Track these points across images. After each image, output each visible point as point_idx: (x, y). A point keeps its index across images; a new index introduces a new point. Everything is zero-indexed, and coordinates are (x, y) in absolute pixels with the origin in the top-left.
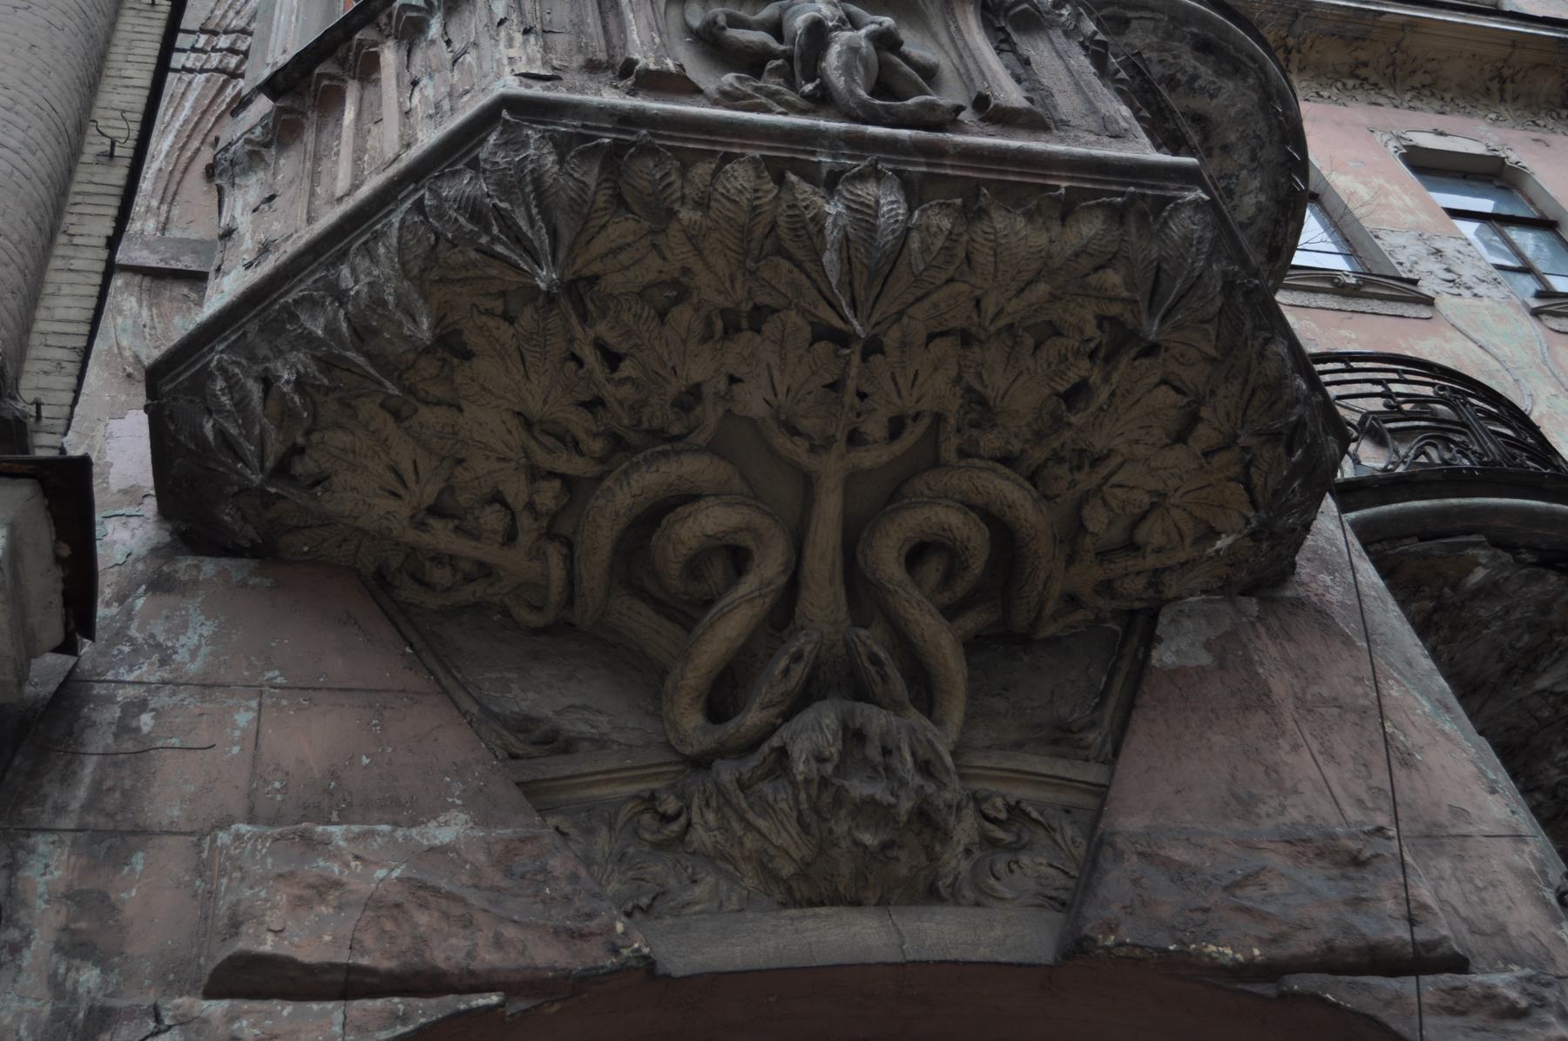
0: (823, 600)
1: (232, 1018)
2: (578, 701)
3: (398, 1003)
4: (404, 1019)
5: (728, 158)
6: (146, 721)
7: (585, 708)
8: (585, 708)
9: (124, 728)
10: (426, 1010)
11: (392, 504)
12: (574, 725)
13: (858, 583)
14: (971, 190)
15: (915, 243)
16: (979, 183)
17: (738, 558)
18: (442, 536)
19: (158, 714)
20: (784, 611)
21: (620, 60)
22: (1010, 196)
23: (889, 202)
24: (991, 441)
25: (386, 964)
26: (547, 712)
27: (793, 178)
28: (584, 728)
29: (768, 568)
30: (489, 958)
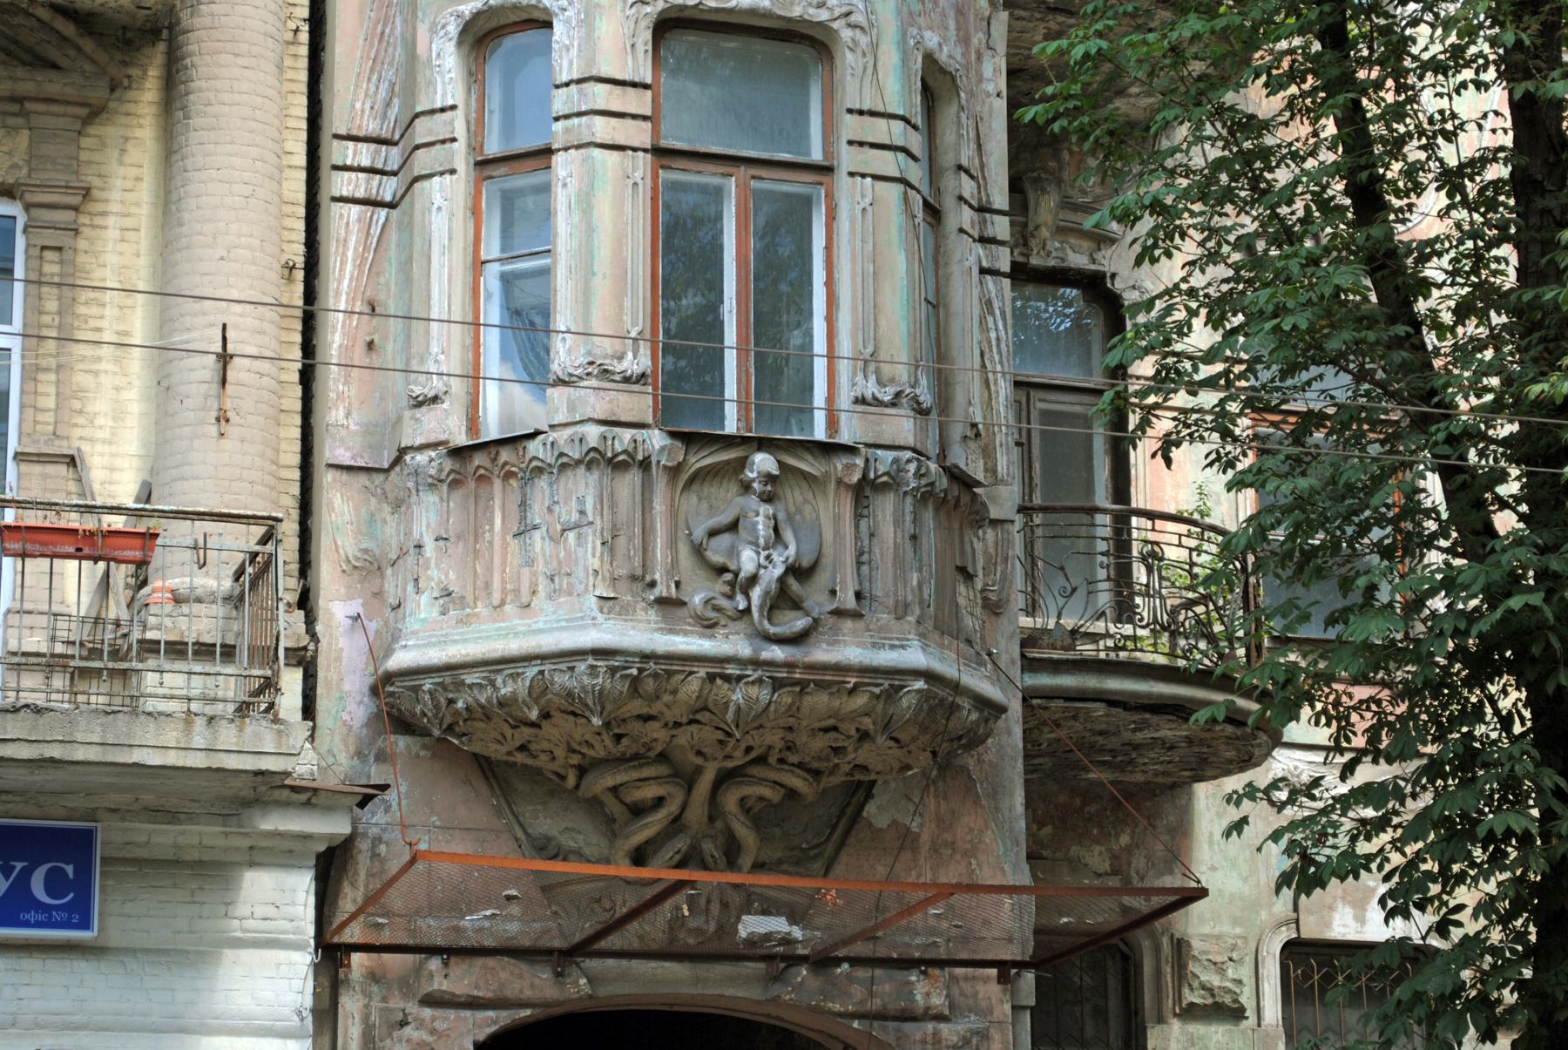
0: (697, 812)
1: (434, 1019)
2: (570, 825)
3: (491, 1013)
4: (494, 1022)
5: (691, 673)
6: (382, 849)
7: (573, 830)
8: (573, 830)
9: (375, 855)
11: (498, 747)
12: (568, 842)
13: (714, 811)
14: (803, 684)
15: (772, 708)
16: (809, 681)
17: (659, 802)
18: (520, 758)
19: (387, 844)
20: (676, 824)
21: (648, 578)
22: (821, 685)
24: (794, 759)
25: (490, 995)
26: (554, 833)
27: (719, 682)
28: (572, 844)
29: (672, 808)
30: (528, 994)
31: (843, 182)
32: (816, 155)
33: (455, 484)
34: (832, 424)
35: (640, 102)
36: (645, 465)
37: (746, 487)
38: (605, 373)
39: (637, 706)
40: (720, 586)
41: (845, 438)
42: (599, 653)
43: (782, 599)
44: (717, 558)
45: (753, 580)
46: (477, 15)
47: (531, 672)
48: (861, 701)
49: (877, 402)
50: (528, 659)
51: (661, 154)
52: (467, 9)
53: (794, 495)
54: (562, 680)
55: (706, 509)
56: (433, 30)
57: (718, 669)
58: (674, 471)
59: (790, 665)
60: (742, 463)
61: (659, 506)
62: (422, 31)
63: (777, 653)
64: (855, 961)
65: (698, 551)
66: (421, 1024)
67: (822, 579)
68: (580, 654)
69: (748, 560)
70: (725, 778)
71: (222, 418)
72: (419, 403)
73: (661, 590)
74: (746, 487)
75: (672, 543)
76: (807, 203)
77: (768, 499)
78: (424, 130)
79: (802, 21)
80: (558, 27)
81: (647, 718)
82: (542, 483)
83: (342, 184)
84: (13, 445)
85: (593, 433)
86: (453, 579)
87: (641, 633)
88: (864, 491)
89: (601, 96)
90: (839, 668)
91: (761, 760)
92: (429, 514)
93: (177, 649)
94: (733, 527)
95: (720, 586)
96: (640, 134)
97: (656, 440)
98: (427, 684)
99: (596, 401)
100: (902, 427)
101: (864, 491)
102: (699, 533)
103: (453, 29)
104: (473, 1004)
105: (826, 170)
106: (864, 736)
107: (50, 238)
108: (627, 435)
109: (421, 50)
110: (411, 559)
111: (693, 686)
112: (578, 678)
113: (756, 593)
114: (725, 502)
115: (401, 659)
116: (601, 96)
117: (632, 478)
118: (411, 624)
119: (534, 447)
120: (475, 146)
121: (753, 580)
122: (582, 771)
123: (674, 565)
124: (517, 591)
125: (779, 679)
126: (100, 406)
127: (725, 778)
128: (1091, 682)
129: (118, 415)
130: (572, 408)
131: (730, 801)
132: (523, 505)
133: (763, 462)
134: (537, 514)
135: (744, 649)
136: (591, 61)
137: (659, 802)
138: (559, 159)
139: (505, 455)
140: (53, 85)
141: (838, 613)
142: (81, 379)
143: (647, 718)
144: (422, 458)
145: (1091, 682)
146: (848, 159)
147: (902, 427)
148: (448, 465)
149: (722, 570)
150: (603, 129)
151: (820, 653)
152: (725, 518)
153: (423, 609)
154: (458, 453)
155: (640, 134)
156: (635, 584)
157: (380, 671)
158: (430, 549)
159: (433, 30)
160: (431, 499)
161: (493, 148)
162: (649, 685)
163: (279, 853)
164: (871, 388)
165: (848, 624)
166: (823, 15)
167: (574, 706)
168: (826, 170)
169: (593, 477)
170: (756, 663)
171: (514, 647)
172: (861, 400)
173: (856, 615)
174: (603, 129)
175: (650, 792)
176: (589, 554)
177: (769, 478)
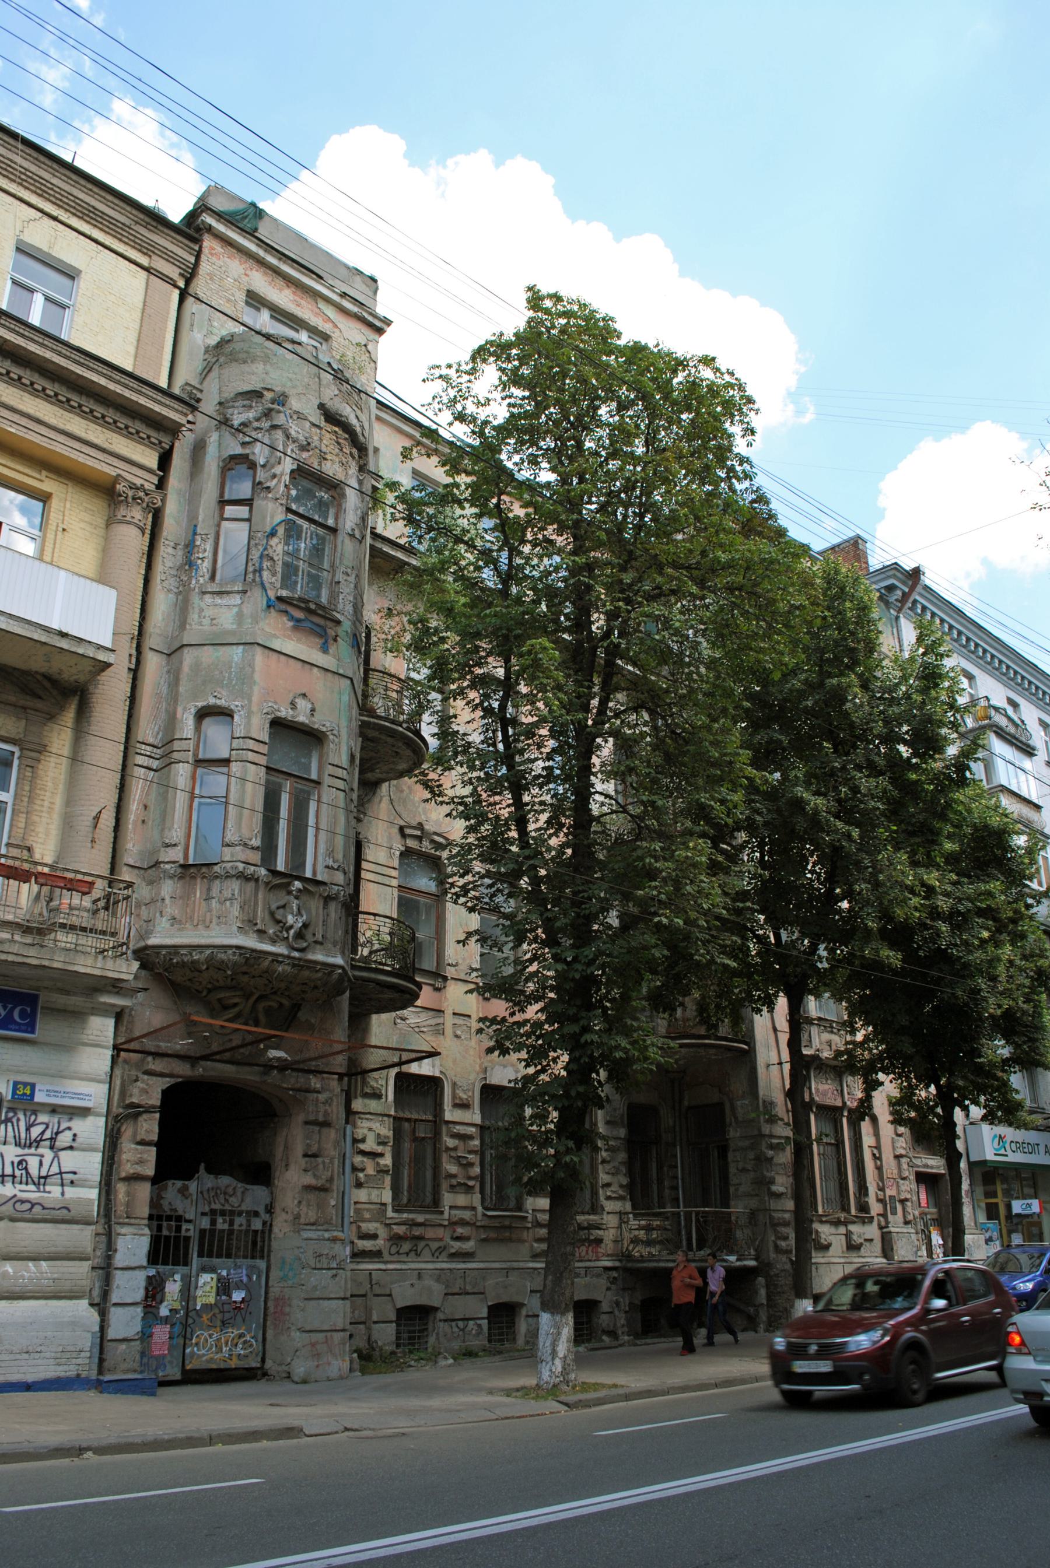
10: (173, 1081)
23: (288, 968)
31: (325, 788)
32: (314, 776)
33: (181, 878)
34: (314, 873)
35: (264, 749)
36: (257, 880)
37: (290, 893)
38: (245, 845)
39: (244, 969)
40: (278, 928)
41: (319, 878)
42: (238, 947)
43: (300, 935)
44: (279, 917)
45: (291, 927)
46: (203, 707)
47: (208, 952)
48: (320, 975)
49: (332, 868)
50: (208, 947)
51: (267, 768)
52: (200, 704)
53: (304, 898)
54: (222, 956)
55: (278, 899)
56: (185, 709)
57: (276, 957)
58: (267, 884)
59: (299, 959)
60: (289, 884)
61: (260, 896)
62: (180, 710)
63: (296, 954)
64: (293, 1070)
65: (272, 914)
66: (143, 1081)
67: (311, 930)
68: (230, 947)
69: (290, 919)
70: (261, 998)
71: (93, 841)
72: (168, 846)
73: (259, 927)
74: (290, 893)
75: (263, 911)
76: (309, 793)
77: (297, 898)
78: (177, 745)
79: (317, 730)
80: (236, 717)
81: (245, 973)
82: (217, 882)
83: (140, 760)
84: (5, 840)
85: (241, 866)
86: (176, 913)
87: (251, 942)
88: (327, 899)
89: (251, 744)
90: (316, 962)
91: (275, 993)
92: (168, 888)
93: (73, 928)
94: (284, 907)
95: (278, 928)
96: (263, 760)
97: (263, 871)
98: (164, 952)
99: (240, 853)
100: (339, 878)
101: (327, 899)
102: (274, 907)
103: (193, 711)
104: (162, 1075)
105: (318, 783)
106: (316, 987)
107: (29, 762)
108: (252, 868)
109: (179, 716)
110: (159, 904)
111: (266, 963)
112: (230, 956)
113: (292, 932)
114: (281, 898)
115: (152, 941)
116: (251, 744)
117: (252, 884)
118: (158, 928)
119: (216, 868)
120: (195, 754)
121: (291, 927)
122: (210, 991)
123: (263, 920)
124: (204, 921)
125: (297, 964)
126: (41, 829)
127: (261, 998)
128: (373, 976)
129: (47, 834)
130: (232, 855)
131: (261, 1006)
132: (209, 890)
133: (298, 884)
134: (215, 892)
135: (285, 952)
136: (249, 731)
137: (235, 1005)
138: (233, 765)
139: (204, 870)
140: (39, 704)
141: (316, 942)
142: (35, 818)
143: (245, 973)
144: (167, 866)
145: (373, 976)
146: (327, 780)
147: (339, 878)
148: (179, 870)
149: (278, 922)
150: (251, 756)
151: (311, 956)
152: (281, 903)
153: (163, 923)
154: (182, 866)
155: (263, 760)
156: (249, 924)
157: (142, 944)
158: (168, 901)
159: (185, 709)
160: (169, 882)
161: (201, 756)
162: (252, 961)
163: (103, 1011)
164: (331, 863)
165: (318, 947)
166: (324, 729)
167: (221, 967)
168: (318, 783)
169: (238, 882)
170: (288, 957)
171: (203, 941)
172: (327, 867)
173: (321, 943)
174: (251, 756)
175: (236, 1000)
176: (235, 911)
177: (299, 890)
